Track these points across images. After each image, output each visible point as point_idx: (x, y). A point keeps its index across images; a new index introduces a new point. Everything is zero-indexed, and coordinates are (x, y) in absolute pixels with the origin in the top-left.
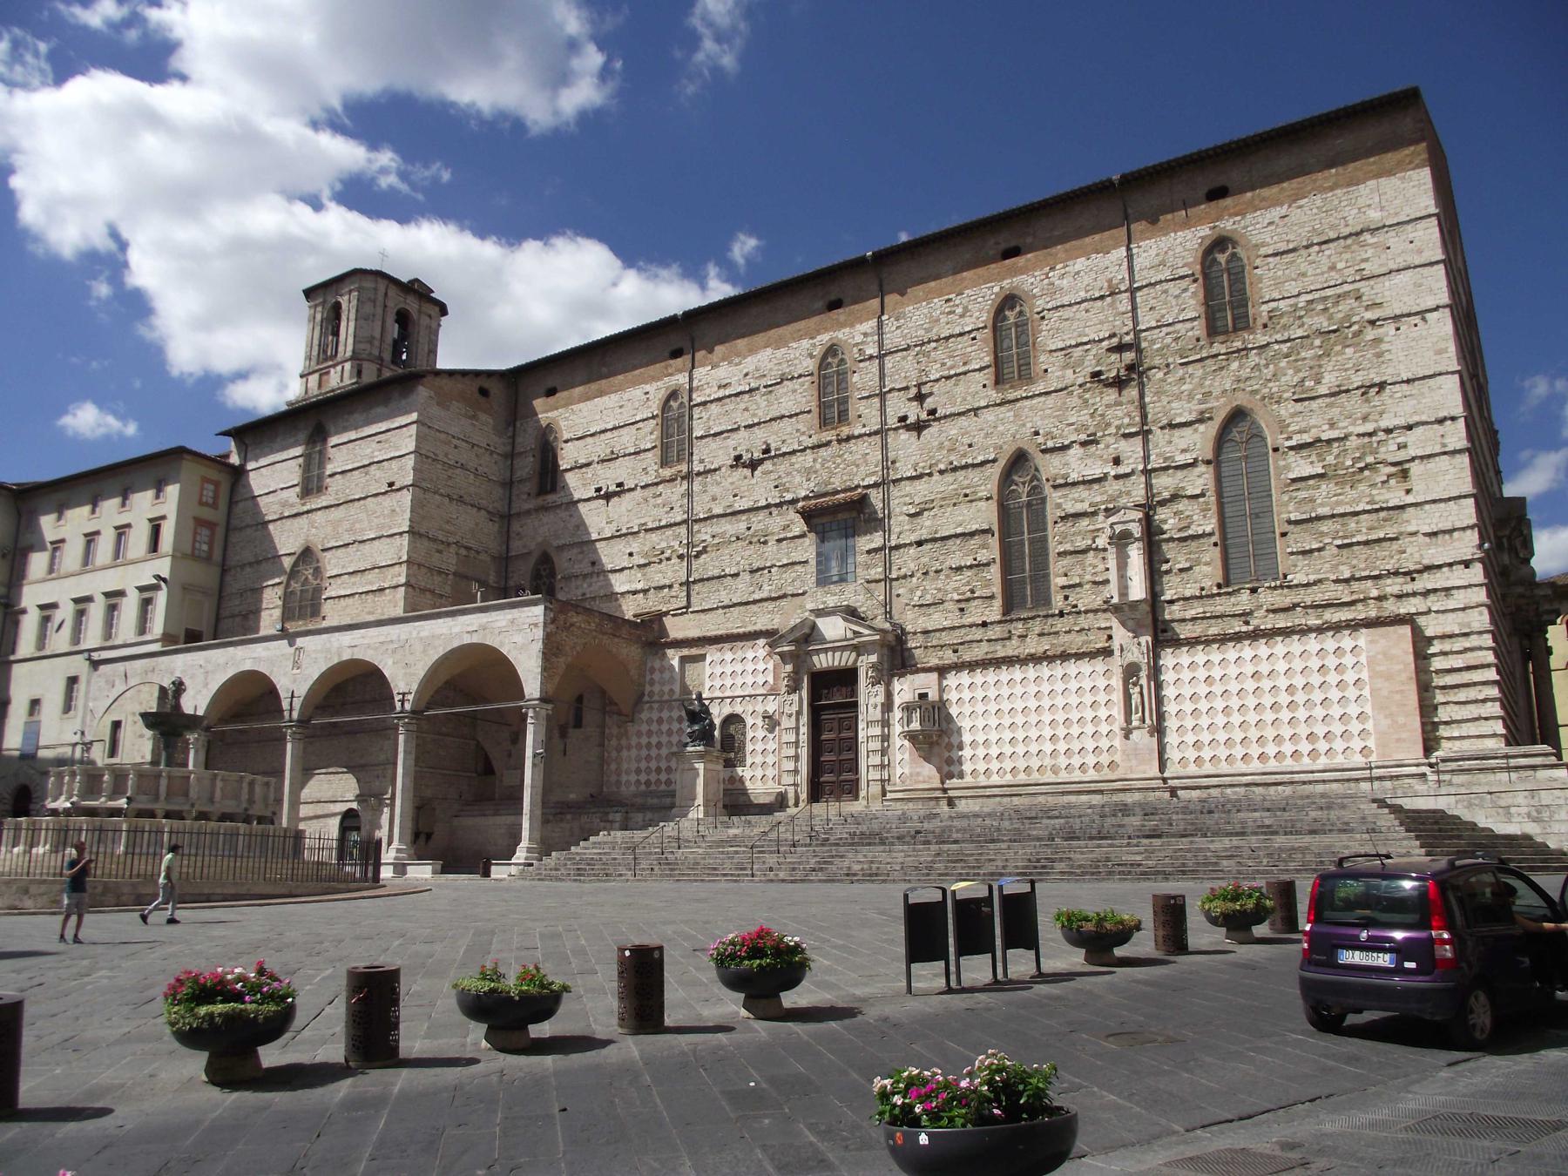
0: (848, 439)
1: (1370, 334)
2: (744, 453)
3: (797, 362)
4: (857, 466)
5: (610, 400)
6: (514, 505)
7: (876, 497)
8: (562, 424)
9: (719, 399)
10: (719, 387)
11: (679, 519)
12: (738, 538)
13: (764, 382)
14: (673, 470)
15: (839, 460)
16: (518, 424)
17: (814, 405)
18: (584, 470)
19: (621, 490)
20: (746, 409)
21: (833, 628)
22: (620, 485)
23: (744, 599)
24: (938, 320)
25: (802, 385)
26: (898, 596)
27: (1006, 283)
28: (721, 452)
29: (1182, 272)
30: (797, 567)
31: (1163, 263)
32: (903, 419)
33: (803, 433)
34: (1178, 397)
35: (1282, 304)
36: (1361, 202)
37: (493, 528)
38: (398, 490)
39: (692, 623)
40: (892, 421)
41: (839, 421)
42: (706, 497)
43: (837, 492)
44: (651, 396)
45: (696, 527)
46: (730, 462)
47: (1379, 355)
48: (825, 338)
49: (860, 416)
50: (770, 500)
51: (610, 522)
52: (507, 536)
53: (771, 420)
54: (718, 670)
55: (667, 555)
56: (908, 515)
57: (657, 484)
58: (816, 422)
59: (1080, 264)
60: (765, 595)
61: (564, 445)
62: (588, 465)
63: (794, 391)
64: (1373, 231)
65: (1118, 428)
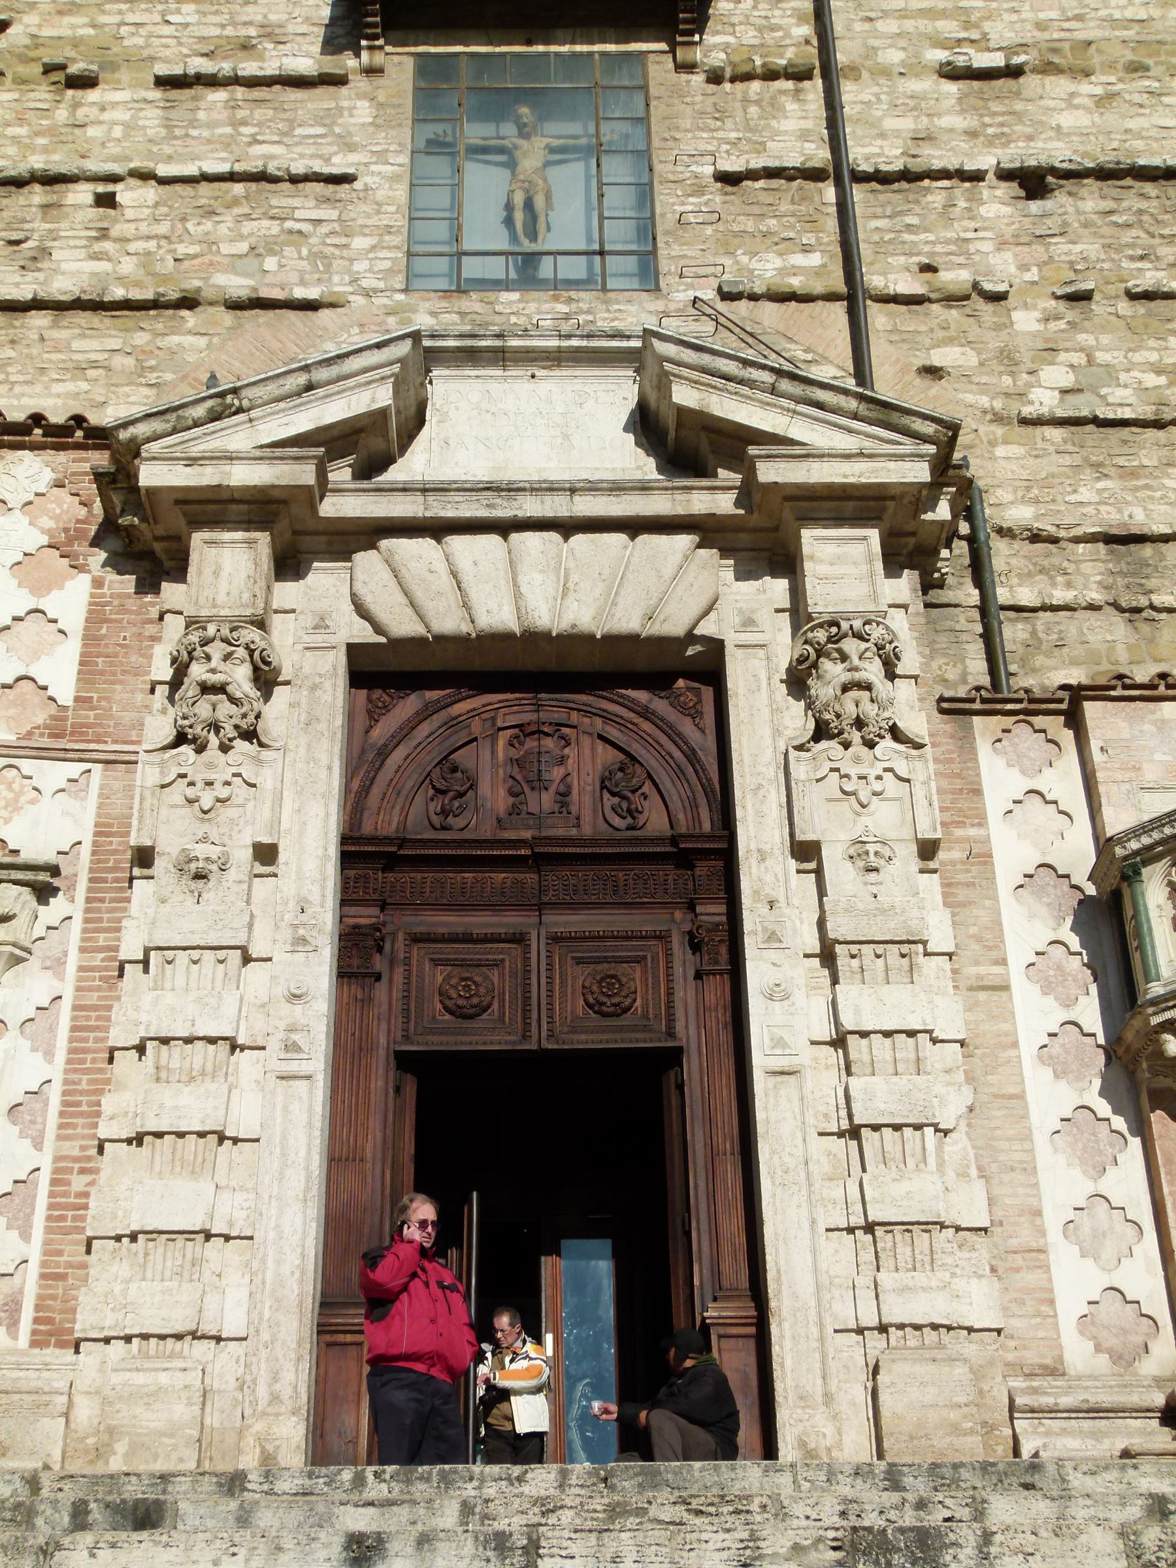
30: (281, 198)
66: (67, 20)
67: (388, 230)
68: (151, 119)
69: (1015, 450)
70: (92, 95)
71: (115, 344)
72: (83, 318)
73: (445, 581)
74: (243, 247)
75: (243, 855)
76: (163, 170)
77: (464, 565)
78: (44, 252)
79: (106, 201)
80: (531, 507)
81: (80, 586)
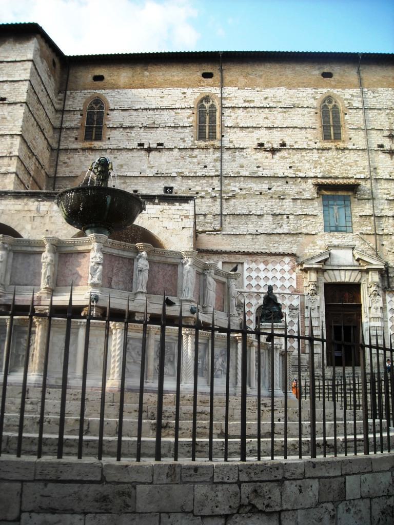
0: (344, 149)
2: (265, 143)
3: (303, 99)
4: (351, 166)
5: (155, 92)
6: (62, 144)
7: (366, 186)
8: (109, 99)
9: (245, 108)
10: (245, 101)
11: (212, 174)
12: (261, 193)
13: (280, 105)
14: (207, 143)
15: (338, 161)
16: (68, 93)
17: (318, 125)
18: (128, 130)
19: (160, 148)
20: (267, 118)
21: (344, 257)
22: (161, 144)
23: (269, 231)
26: (383, 245)
28: (246, 139)
30: (309, 218)
32: (381, 146)
33: (311, 140)
37: (47, 154)
38: (10, 104)
39: (224, 241)
40: (375, 147)
41: (335, 139)
42: (235, 165)
43: (337, 178)
44: (188, 95)
45: (226, 182)
46: (254, 146)
48: (325, 91)
49: (350, 139)
50: (286, 174)
51: (152, 167)
52: (56, 164)
53: (286, 127)
54: (254, 274)
55: (203, 194)
56: (387, 200)
57: (193, 149)
58: (320, 136)
60: (286, 231)
61: (109, 112)
62: (131, 128)
63: (304, 115)
66: (279, 188)
67: (321, 223)
68: (291, 204)
69: (392, 256)
70: (284, 201)
71: (292, 239)
72: (288, 235)
73: (333, 276)
74: (305, 225)
75: (317, 307)
76: (295, 214)
77: (336, 274)
78: (282, 225)
79: (288, 218)
80: (343, 268)
81: (295, 273)
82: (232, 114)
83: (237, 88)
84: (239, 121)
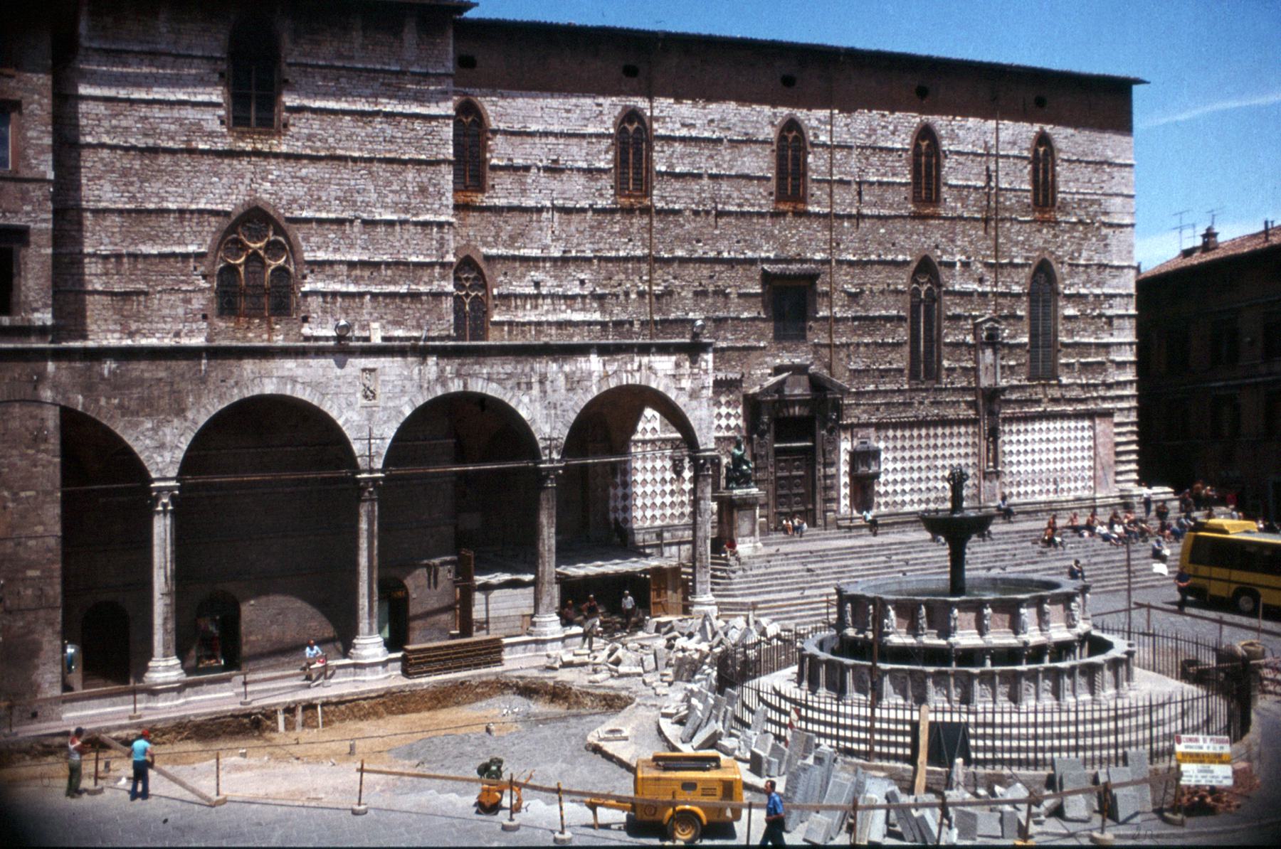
1: (1104, 231)
9: (683, 139)
10: (684, 125)
20: (711, 157)
24: (875, 130)
25: (764, 150)
27: (924, 117)
29: (1025, 154)
31: (1014, 143)
34: (1016, 243)
35: (1069, 197)
36: (1106, 142)
47: (1106, 245)
48: (784, 111)
59: (971, 122)
64: (1110, 164)
65: (984, 256)
82: (666, 148)
83: (672, 101)
84: (674, 161)
